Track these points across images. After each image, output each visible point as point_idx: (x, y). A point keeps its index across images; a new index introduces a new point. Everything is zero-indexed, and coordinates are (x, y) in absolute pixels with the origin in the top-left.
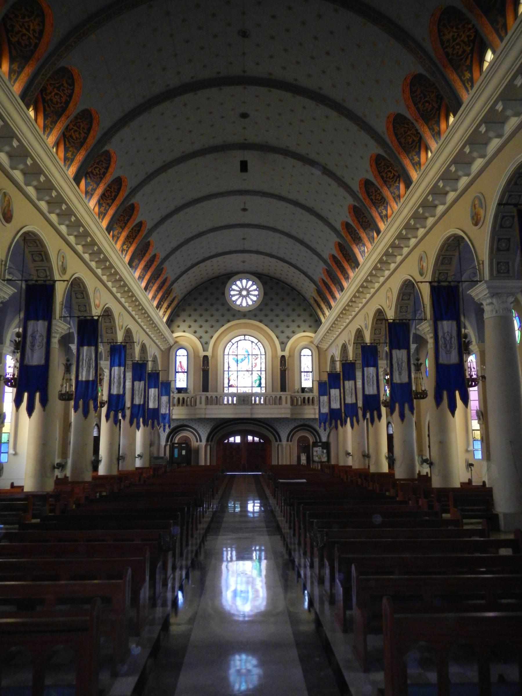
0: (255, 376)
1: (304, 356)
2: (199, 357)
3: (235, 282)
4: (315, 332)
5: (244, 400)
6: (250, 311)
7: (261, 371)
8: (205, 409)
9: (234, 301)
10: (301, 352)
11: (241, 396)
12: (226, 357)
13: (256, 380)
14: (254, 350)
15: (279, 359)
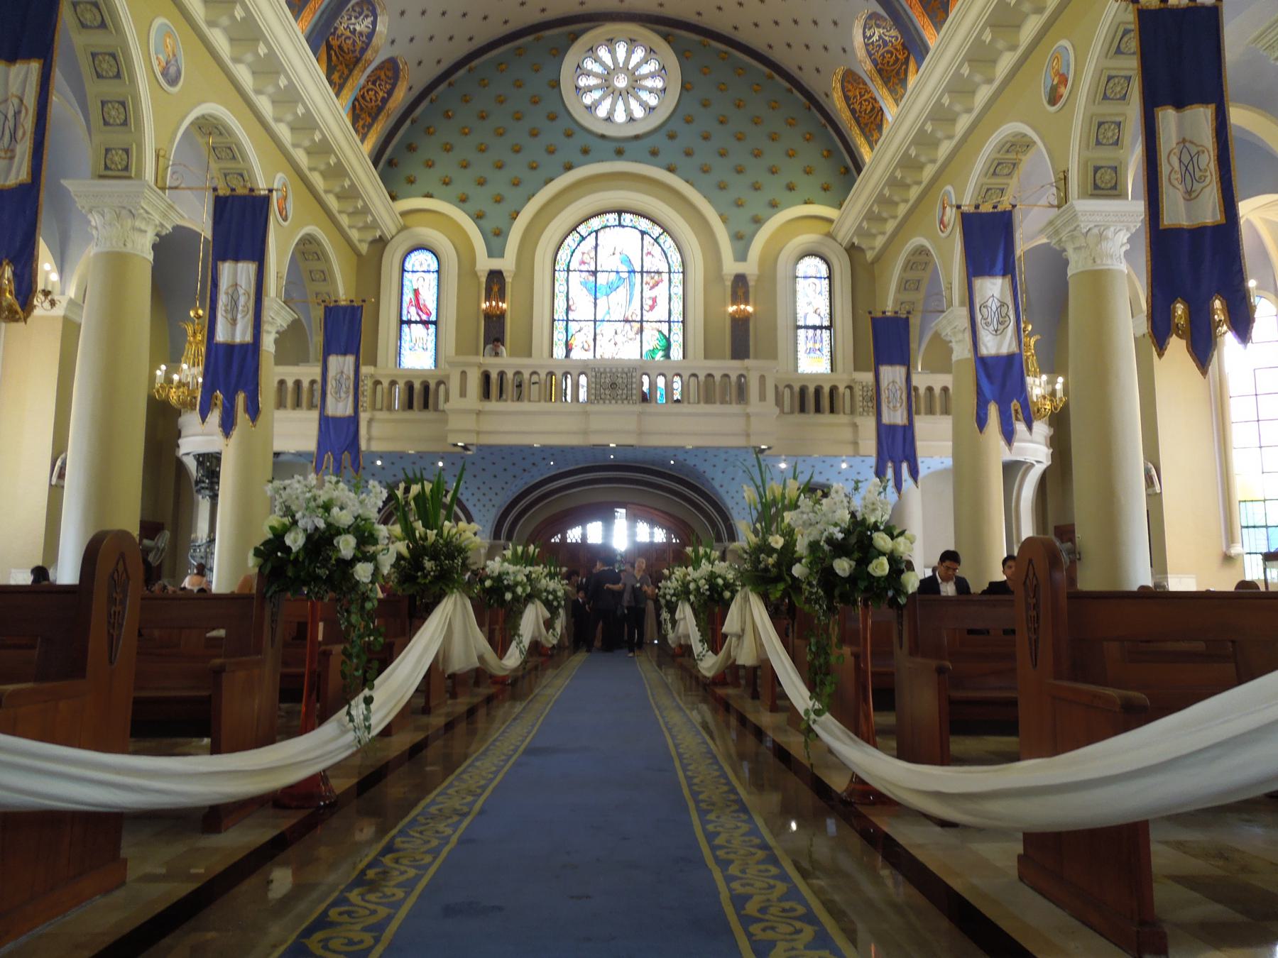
0: (651, 339)
1: (805, 277)
2: (475, 274)
3: (592, 50)
4: (840, 206)
5: (613, 386)
6: (637, 137)
7: (669, 322)
8: (479, 413)
9: (588, 108)
10: (795, 269)
11: (605, 372)
12: (561, 276)
13: (653, 351)
14: (647, 259)
15: (729, 284)
